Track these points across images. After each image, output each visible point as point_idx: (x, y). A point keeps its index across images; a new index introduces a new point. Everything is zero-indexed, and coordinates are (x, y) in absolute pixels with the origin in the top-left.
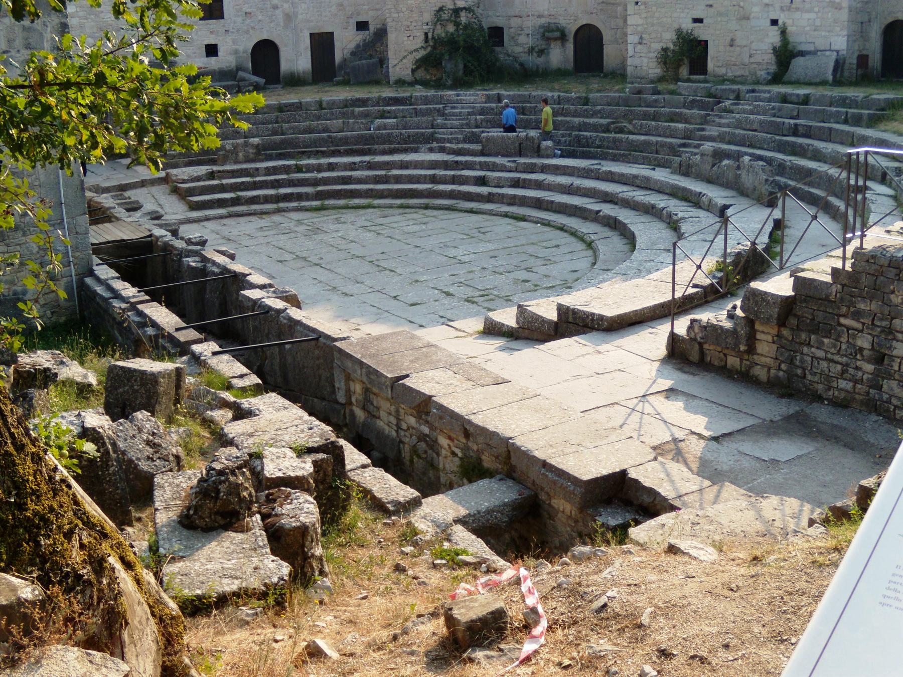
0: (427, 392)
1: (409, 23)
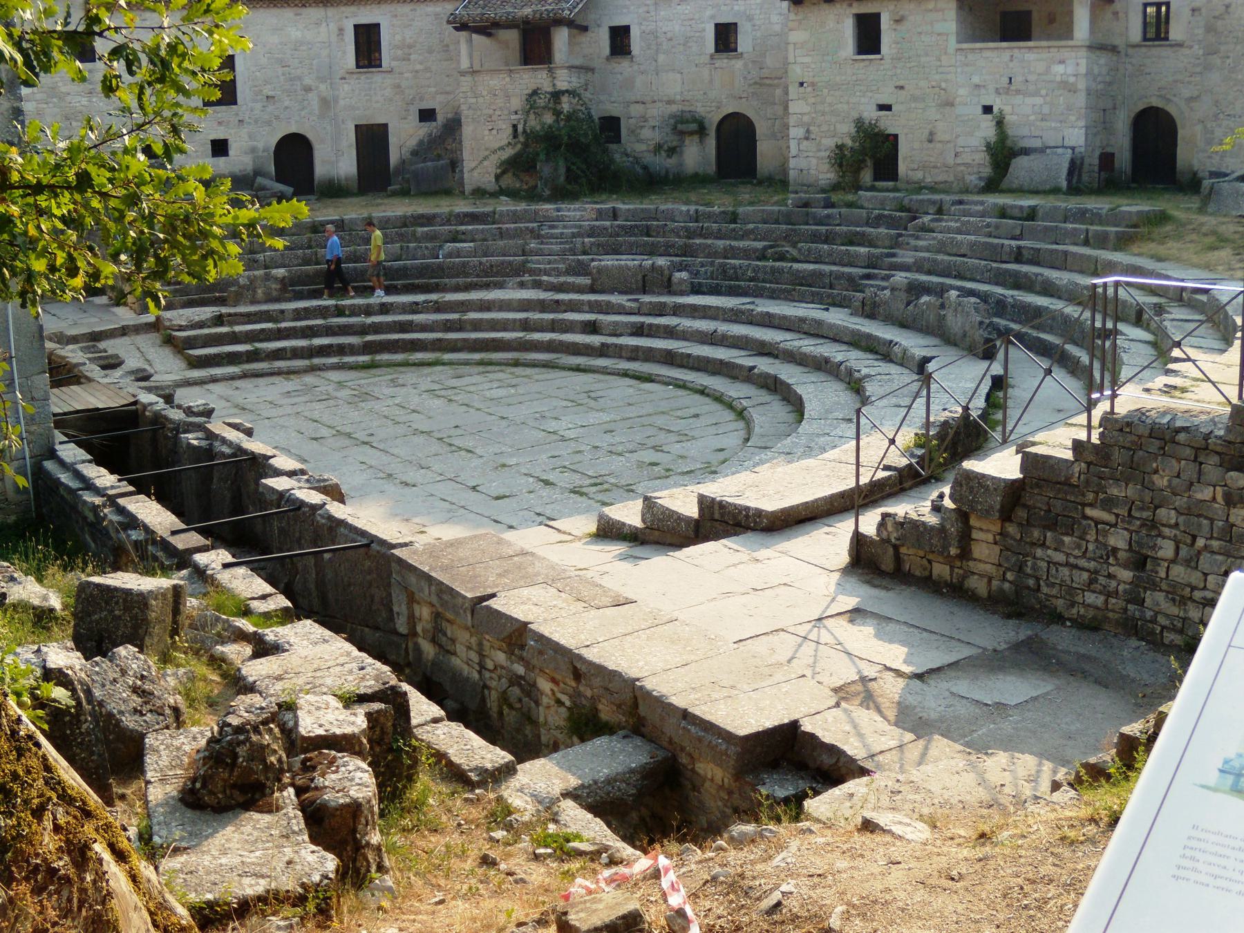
0: (522, 617)
1: (491, 112)
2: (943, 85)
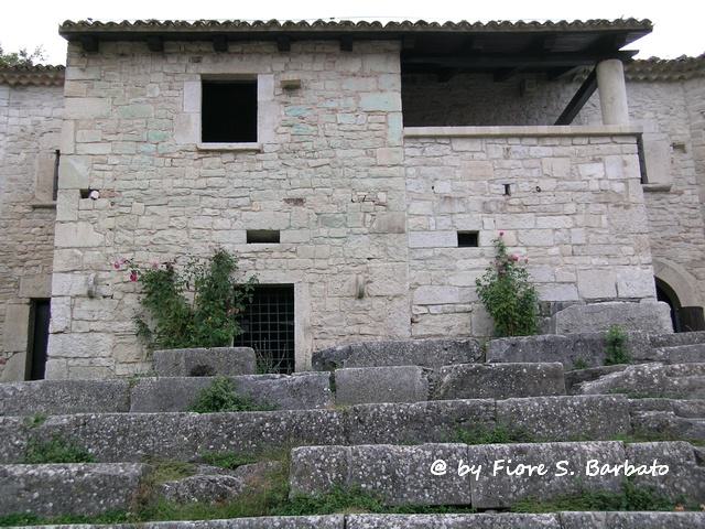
2: (382, 197)
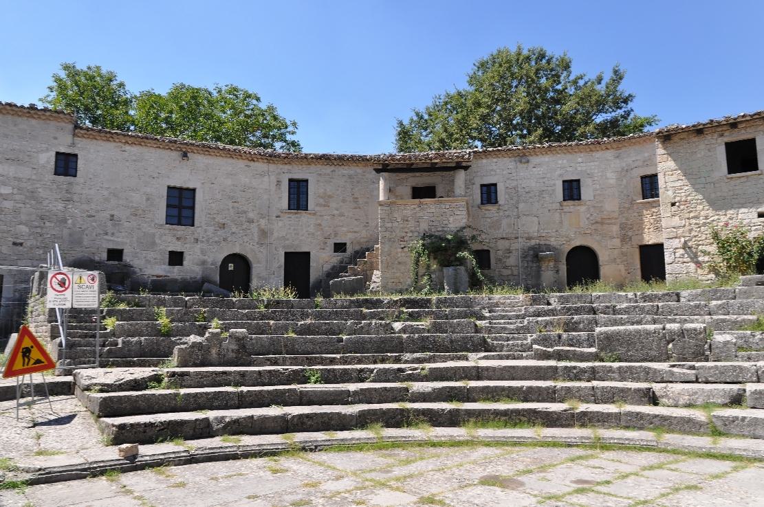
1: (404, 234)
